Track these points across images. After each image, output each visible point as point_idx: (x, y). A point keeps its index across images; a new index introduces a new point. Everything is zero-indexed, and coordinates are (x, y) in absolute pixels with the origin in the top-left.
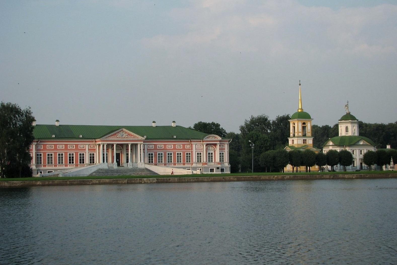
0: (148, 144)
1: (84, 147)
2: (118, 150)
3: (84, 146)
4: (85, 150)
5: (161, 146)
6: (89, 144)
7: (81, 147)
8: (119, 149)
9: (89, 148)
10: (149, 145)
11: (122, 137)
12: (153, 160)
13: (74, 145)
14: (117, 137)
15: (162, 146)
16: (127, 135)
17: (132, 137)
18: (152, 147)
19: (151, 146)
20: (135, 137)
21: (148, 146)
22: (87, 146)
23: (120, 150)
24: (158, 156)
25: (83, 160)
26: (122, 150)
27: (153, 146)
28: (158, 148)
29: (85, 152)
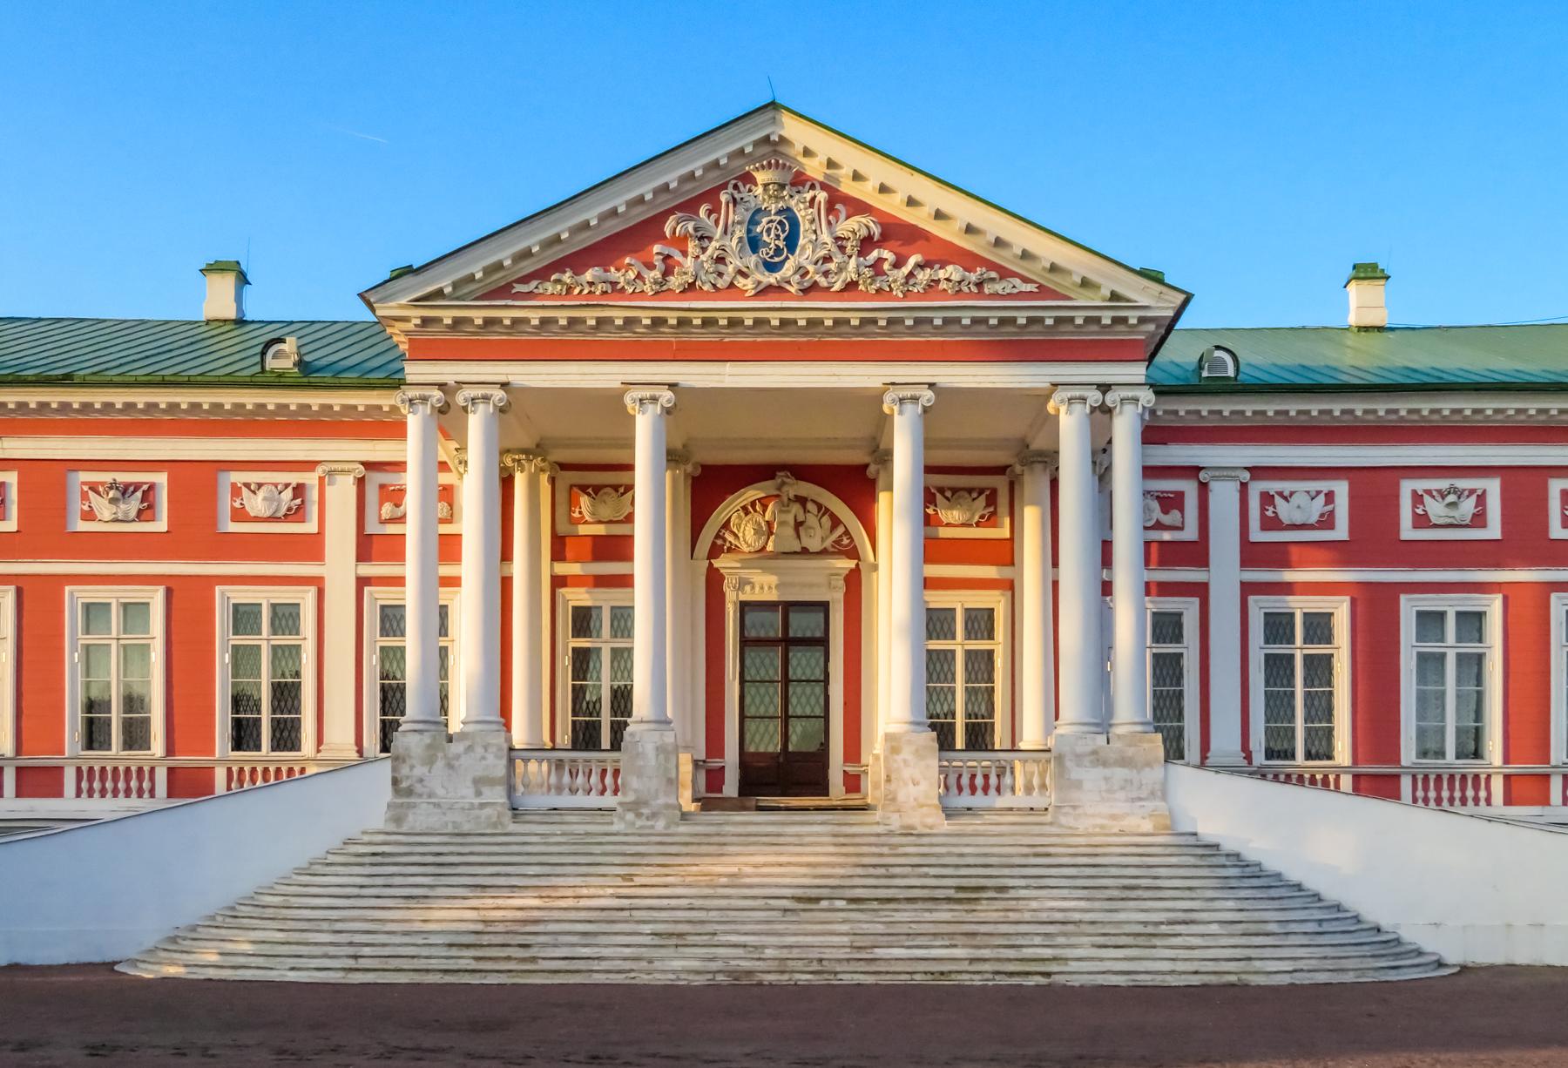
0: (1258, 472)
1: (297, 514)
2: (805, 552)
3: (299, 490)
4: (312, 547)
5: (1468, 507)
6: (369, 466)
7: (257, 504)
8: (814, 544)
9: (372, 528)
10: (1273, 486)
11: (772, 279)
12: (1329, 714)
13: (161, 479)
14: (675, 282)
15: (1481, 499)
16: (867, 244)
17: (953, 272)
18: (1317, 508)
19: (1300, 503)
20: (1005, 273)
21: (1267, 499)
22: (342, 494)
23: (824, 553)
24: (1422, 658)
25: (286, 695)
26: (853, 553)
27: (1330, 497)
28: (1407, 532)
29: (318, 582)
